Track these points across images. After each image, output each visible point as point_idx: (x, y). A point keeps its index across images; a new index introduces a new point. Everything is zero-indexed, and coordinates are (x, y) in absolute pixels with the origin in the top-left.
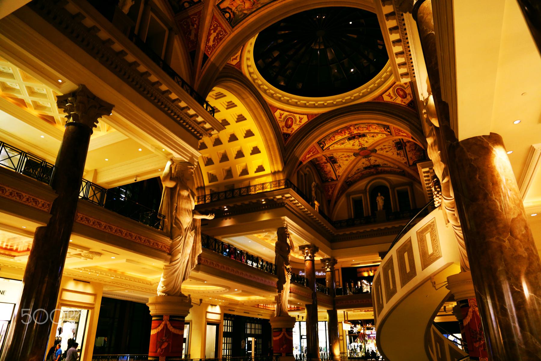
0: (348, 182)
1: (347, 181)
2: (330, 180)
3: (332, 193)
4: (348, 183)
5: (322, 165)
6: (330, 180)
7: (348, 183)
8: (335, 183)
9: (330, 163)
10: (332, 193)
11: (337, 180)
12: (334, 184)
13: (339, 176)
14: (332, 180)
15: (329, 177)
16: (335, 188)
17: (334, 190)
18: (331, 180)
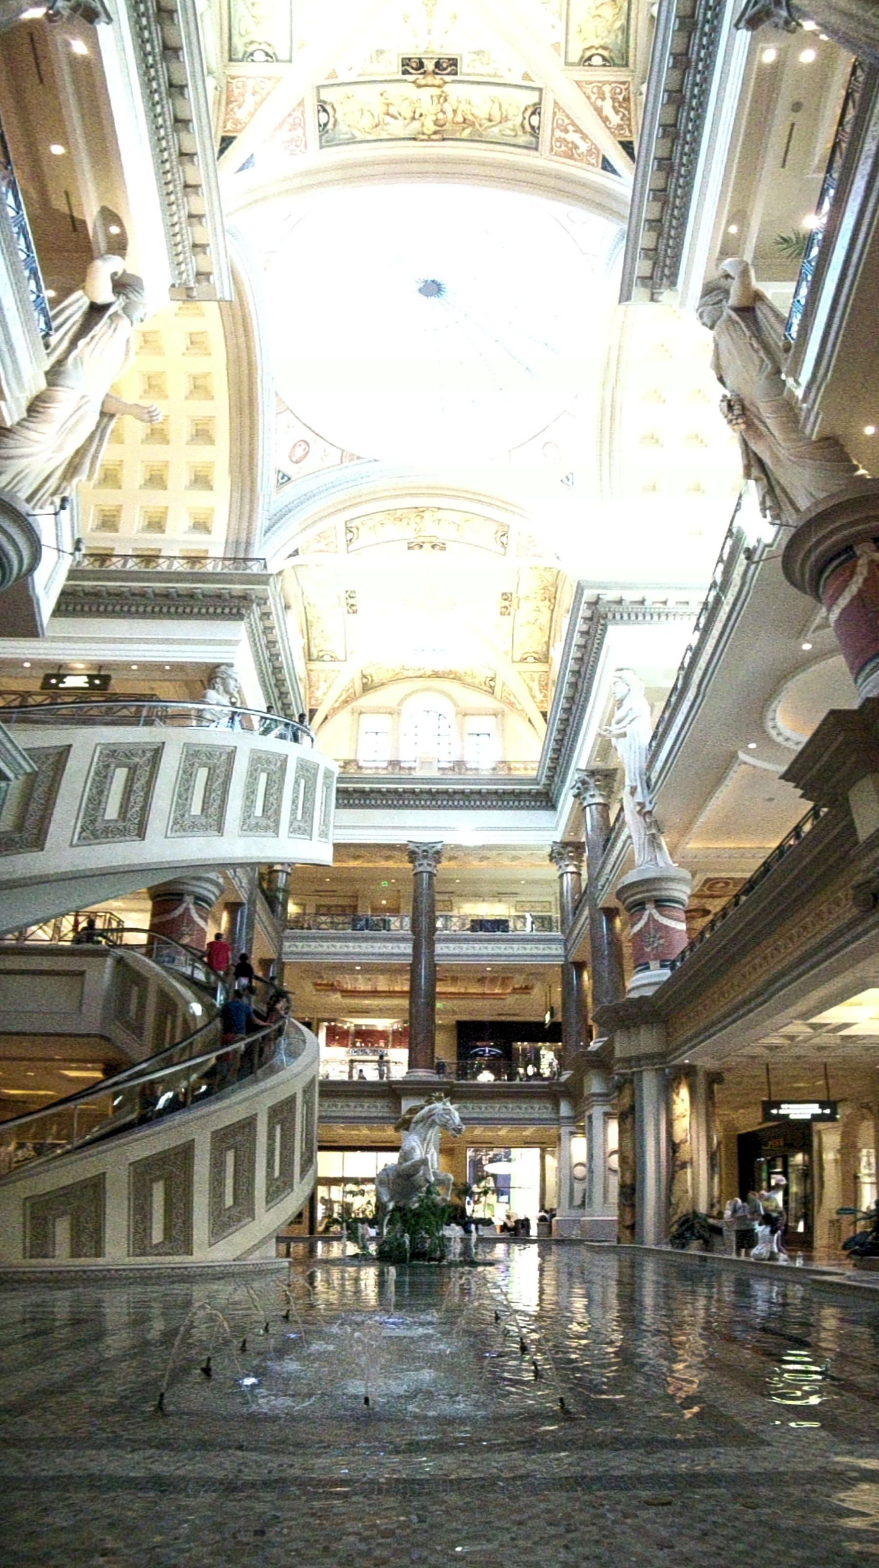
0: (586, 61)
1: (574, 57)
2: (535, 120)
3: (584, 137)
4: (597, 61)
5: (450, 115)
6: (535, 120)
7: (597, 61)
8: (547, 109)
9: (445, 83)
10: (584, 137)
11: (540, 90)
12: (555, 113)
13: (526, 76)
14: (536, 110)
15: (520, 118)
16: (568, 117)
17: (573, 124)
18: (533, 113)
